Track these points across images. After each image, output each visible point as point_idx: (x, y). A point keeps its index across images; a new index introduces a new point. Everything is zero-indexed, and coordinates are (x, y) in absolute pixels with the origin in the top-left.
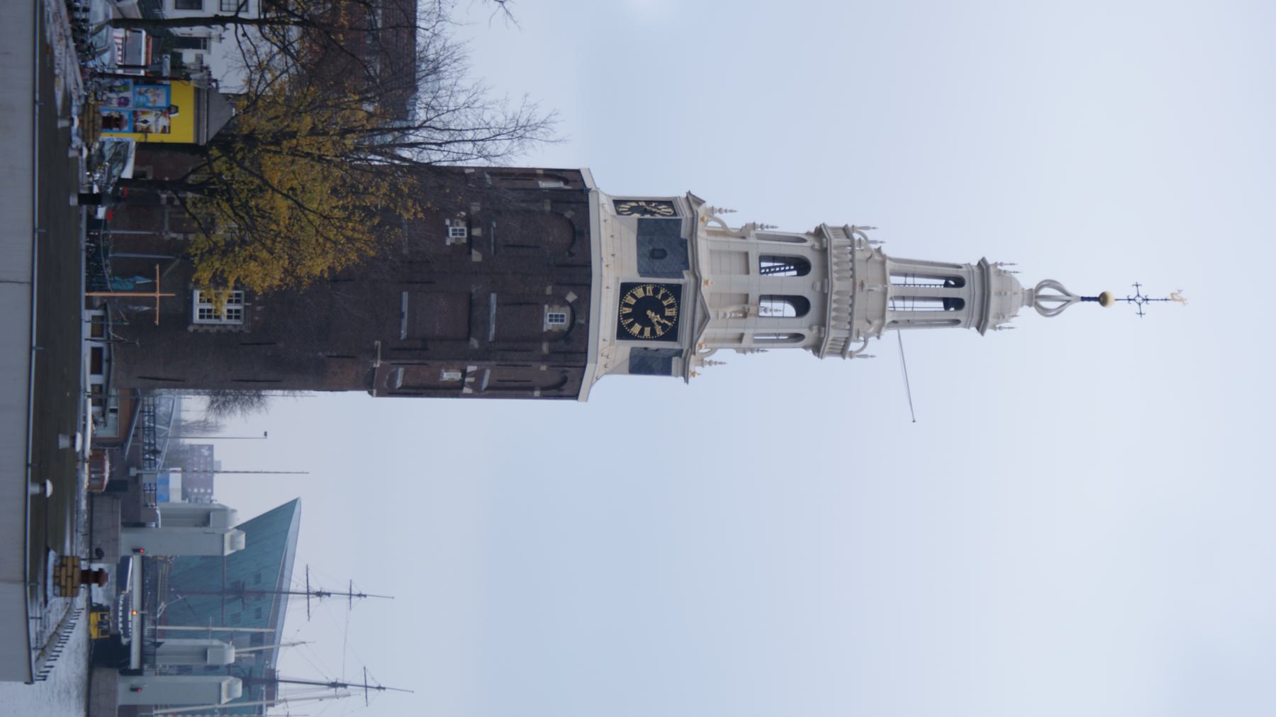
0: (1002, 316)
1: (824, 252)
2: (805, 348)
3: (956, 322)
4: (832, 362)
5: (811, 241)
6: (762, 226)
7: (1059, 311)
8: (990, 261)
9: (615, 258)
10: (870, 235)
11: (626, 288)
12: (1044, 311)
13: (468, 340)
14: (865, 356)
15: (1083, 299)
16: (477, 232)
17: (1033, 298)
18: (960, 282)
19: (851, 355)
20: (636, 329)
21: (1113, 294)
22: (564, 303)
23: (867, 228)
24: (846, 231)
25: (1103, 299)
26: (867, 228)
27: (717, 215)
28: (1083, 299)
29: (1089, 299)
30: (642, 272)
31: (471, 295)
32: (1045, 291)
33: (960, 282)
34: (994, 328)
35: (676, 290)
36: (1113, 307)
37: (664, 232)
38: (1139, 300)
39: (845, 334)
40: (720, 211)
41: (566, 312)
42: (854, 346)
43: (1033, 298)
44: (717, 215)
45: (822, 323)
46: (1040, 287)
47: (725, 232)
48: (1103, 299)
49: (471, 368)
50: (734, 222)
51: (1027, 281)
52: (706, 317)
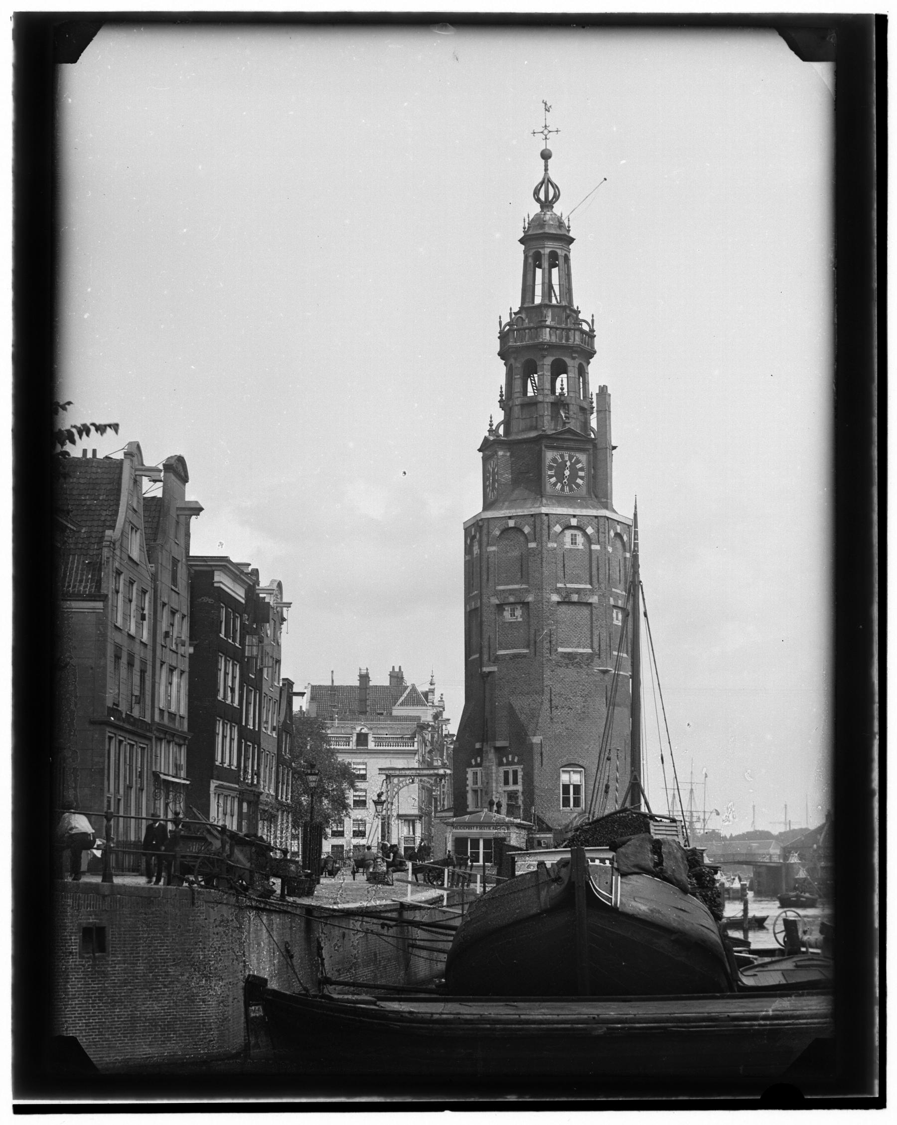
0: (561, 224)
1: (518, 350)
2: (589, 363)
3: (567, 259)
4: (598, 344)
6: (501, 396)
7: (555, 187)
10: (506, 320)
12: (556, 197)
13: (591, 604)
14: (593, 321)
15: (546, 170)
17: (547, 205)
19: (592, 331)
23: (500, 323)
25: (546, 156)
26: (500, 323)
27: (494, 427)
28: (546, 170)
31: (559, 603)
32: (542, 196)
34: (569, 231)
38: (546, 132)
39: (577, 333)
40: (491, 425)
41: (568, 533)
42: (585, 327)
44: (494, 427)
45: (571, 350)
46: (538, 200)
47: (507, 423)
48: (546, 156)
49: (612, 602)
50: (499, 416)
51: (536, 208)
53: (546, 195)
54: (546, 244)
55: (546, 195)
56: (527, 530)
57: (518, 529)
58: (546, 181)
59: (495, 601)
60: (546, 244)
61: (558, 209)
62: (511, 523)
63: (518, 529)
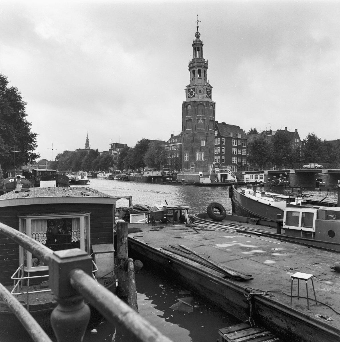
3: (202, 48)
5: (192, 70)
9: (200, 97)
11: (206, 97)
15: (198, 30)
16: (201, 118)
18: (198, 48)
20: (210, 96)
22: (210, 106)
25: (198, 27)
28: (198, 30)
29: (198, 29)
30: (204, 94)
33: (198, 48)
35: (207, 89)
36: (199, 25)
37: (190, 91)
48: (198, 27)
51: (195, 38)
52: (209, 85)
53: (198, 35)
55: (198, 35)
57: (202, 104)
59: (197, 118)
62: (201, 103)
63: (202, 104)
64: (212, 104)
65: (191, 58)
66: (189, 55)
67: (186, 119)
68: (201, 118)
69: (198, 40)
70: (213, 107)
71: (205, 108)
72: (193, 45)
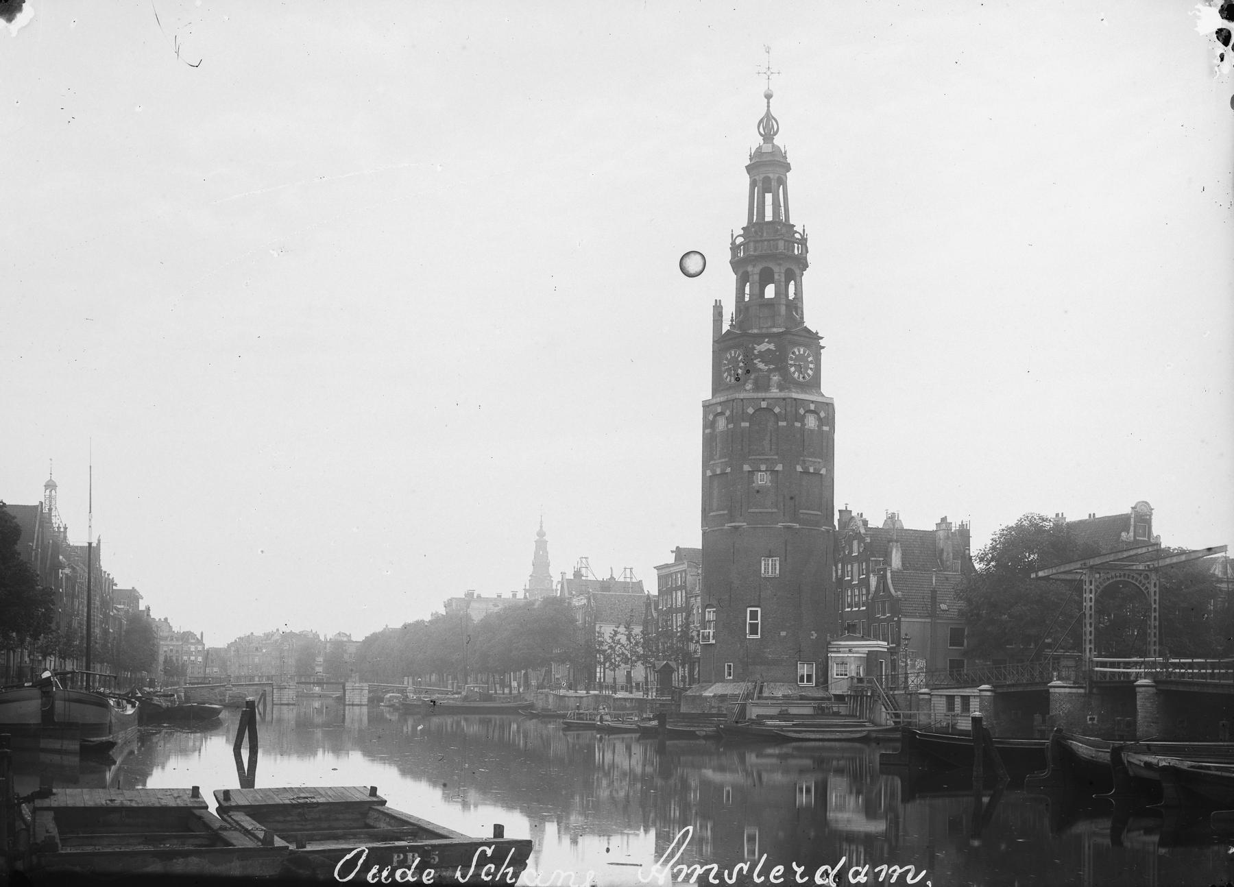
8: (748, 162)
17: (768, 136)
21: (763, 90)
22: (804, 416)
24: (734, 248)
25: (768, 97)
33: (767, 180)
43: (768, 136)
48: (768, 97)
54: (768, 171)
56: (777, 410)
57: (769, 409)
58: (768, 116)
59: (746, 468)
60: (768, 171)
61: (777, 141)
62: (764, 404)
64: (812, 407)
65: (740, 220)
66: (726, 214)
67: (709, 473)
68: (763, 467)
69: (767, 148)
70: (820, 419)
71: (781, 424)
72: (749, 169)
